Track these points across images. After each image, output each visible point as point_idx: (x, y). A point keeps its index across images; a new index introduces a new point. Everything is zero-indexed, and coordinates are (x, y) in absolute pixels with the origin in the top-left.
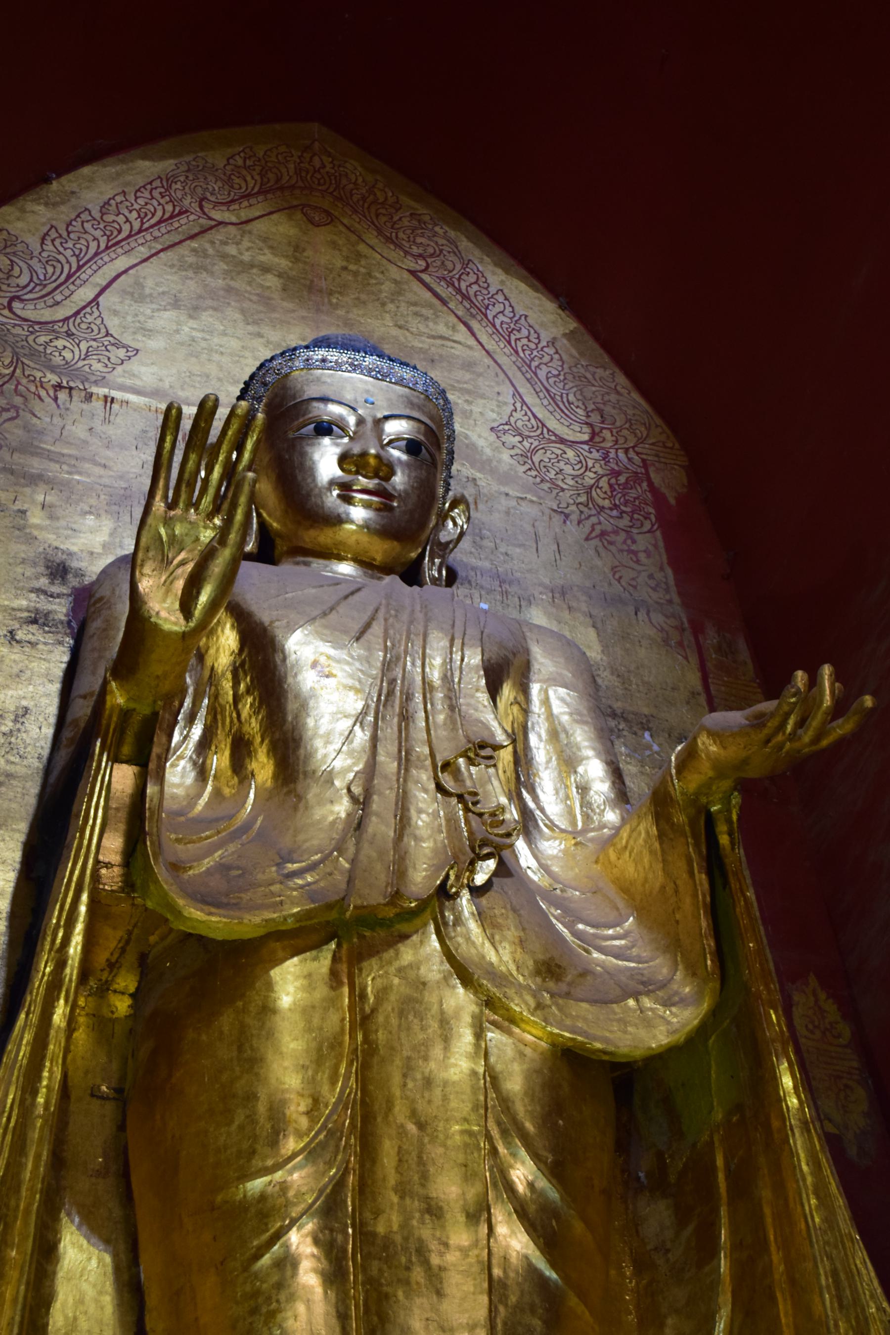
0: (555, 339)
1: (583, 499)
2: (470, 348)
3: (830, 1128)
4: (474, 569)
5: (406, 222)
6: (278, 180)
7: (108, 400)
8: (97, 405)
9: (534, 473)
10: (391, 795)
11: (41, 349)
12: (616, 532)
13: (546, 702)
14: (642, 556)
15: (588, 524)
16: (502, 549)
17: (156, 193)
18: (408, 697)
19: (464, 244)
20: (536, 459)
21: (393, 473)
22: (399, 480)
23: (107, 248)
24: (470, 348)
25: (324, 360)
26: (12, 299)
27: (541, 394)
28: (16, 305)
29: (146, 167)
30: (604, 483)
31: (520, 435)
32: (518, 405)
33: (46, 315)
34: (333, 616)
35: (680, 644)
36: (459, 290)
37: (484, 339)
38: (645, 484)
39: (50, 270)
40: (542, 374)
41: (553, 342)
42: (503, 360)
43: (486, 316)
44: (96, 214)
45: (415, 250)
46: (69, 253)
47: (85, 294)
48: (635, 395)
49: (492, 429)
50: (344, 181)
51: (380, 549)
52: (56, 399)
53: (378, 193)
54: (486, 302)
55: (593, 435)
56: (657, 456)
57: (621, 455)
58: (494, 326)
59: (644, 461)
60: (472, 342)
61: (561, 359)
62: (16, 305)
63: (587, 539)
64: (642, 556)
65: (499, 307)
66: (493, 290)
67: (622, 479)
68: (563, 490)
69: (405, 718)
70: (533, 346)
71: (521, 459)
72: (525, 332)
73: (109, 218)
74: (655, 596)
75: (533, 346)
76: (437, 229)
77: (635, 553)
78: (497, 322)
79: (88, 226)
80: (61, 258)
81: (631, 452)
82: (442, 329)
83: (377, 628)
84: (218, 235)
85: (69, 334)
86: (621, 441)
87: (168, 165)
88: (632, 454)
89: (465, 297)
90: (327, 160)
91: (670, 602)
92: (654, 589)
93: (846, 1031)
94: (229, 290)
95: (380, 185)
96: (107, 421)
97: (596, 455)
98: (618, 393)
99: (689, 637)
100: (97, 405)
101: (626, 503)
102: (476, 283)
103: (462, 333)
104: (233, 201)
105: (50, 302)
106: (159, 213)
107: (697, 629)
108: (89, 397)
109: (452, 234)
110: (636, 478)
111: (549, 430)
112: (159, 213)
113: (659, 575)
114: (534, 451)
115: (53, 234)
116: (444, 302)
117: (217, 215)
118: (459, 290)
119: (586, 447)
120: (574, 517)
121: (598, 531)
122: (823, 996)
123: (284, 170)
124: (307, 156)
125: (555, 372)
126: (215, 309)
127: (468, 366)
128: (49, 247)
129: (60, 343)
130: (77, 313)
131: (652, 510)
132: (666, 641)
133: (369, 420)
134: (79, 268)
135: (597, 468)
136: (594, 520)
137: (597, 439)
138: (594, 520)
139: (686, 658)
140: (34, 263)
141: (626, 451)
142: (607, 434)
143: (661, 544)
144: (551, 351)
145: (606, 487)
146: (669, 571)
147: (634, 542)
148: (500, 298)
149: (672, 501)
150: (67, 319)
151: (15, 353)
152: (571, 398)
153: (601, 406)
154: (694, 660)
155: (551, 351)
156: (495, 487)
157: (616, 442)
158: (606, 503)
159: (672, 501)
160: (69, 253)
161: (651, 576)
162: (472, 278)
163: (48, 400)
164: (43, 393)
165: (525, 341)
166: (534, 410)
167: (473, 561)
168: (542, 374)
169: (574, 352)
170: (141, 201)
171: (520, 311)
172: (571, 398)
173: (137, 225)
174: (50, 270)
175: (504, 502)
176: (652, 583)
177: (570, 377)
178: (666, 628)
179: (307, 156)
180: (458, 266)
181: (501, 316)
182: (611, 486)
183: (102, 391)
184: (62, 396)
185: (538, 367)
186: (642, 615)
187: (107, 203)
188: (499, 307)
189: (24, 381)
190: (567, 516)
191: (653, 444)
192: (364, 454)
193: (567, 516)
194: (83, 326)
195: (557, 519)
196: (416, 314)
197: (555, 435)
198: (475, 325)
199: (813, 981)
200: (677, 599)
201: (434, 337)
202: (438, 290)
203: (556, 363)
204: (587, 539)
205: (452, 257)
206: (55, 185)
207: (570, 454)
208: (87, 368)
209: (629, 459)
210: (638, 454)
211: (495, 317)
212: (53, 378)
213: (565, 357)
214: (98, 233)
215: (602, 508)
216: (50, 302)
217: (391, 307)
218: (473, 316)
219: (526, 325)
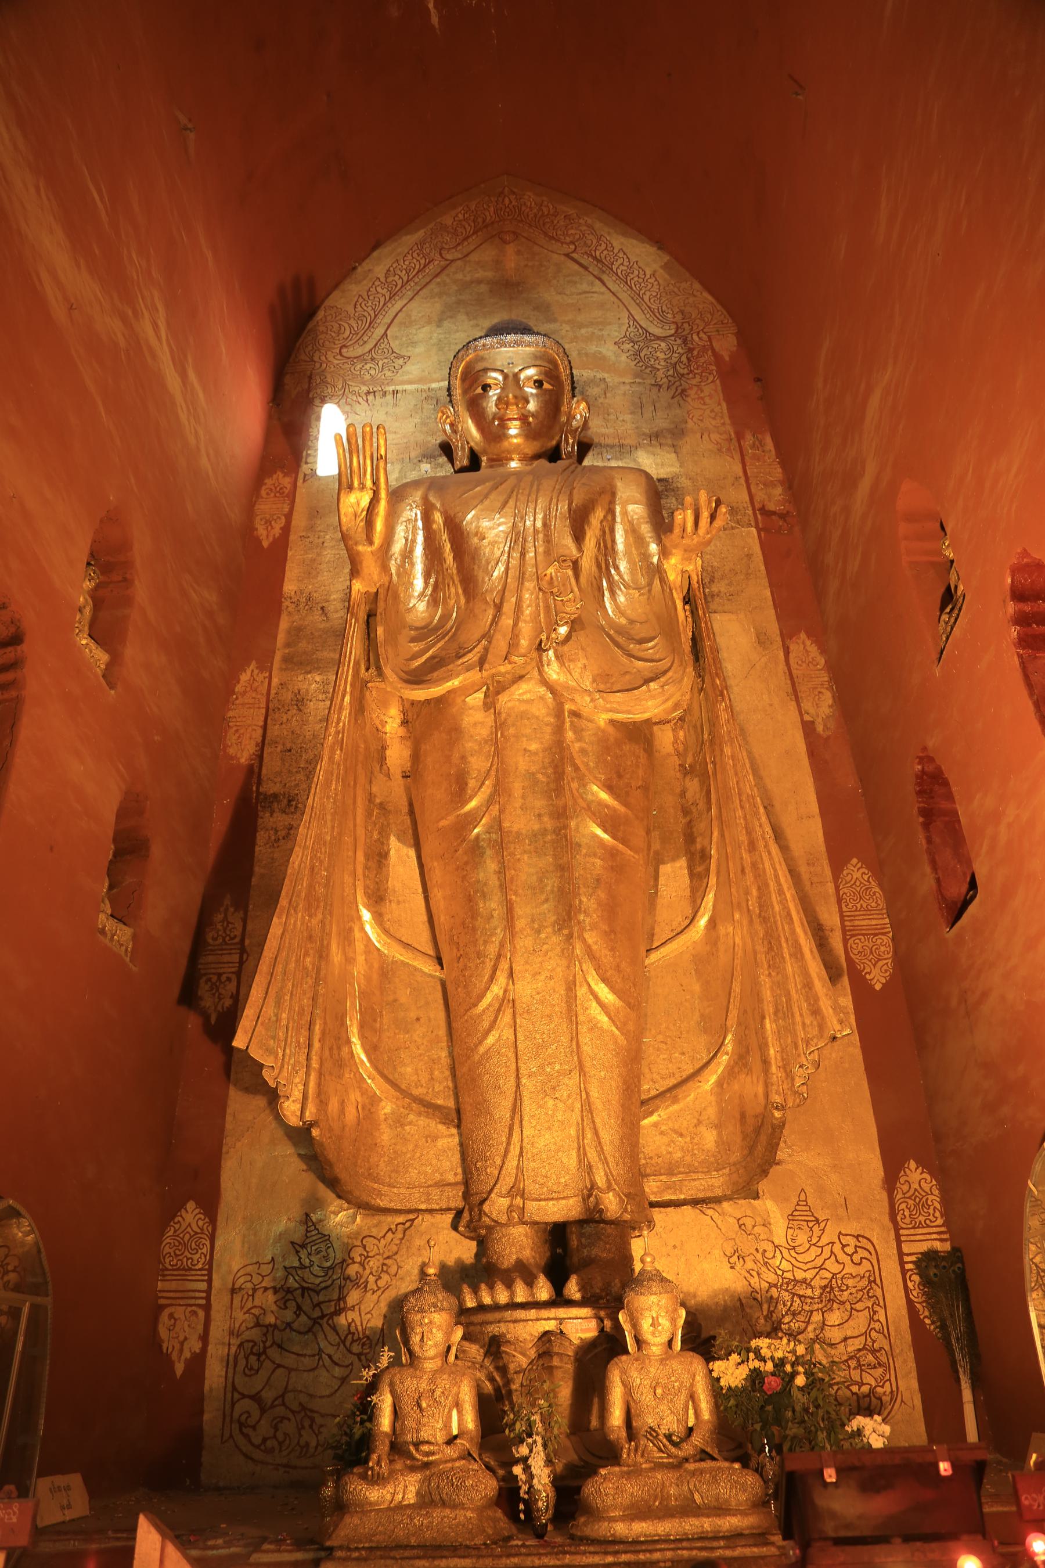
0: (655, 271)
1: (671, 372)
2: (603, 293)
3: (807, 718)
4: (603, 435)
5: (562, 223)
6: (484, 221)
7: (395, 393)
8: (389, 397)
10: (514, 600)
12: (691, 388)
13: (625, 513)
14: (707, 400)
15: (673, 388)
16: (621, 419)
17: (415, 255)
18: (525, 541)
19: (598, 225)
20: (642, 355)
21: (528, 402)
22: (532, 406)
24: (603, 293)
25: (484, 345)
26: (341, 348)
29: (409, 240)
30: (684, 359)
33: (360, 351)
34: (487, 502)
35: (729, 449)
36: (595, 258)
37: (610, 285)
38: (710, 352)
39: (360, 323)
40: (646, 298)
41: (653, 275)
42: (623, 296)
44: (383, 280)
45: (568, 240)
47: (379, 332)
48: (706, 294)
50: (523, 208)
53: (544, 209)
55: (677, 329)
57: (695, 337)
58: (617, 274)
59: (709, 337)
60: (604, 289)
62: (344, 350)
63: (673, 398)
64: (707, 400)
65: (620, 261)
66: (616, 251)
67: (695, 353)
69: (523, 554)
70: (641, 280)
72: (636, 272)
73: (390, 279)
74: (714, 422)
75: (641, 280)
76: (581, 221)
77: (702, 398)
78: (619, 271)
79: (379, 289)
80: (366, 314)
82: (585, 287)
83: (511, 503)
84: (452, 269)
85: (373, 359)
86: (695, 327)
87: (421, 234)
88: (702, 335)
89: (599, 261)
90: (513, 197)
91: (724, 424)
92: (714, 418)
93: (823, 661)
94: (459, 302)
95: (545, 203)
96: (395, 405)
97: (679, 341)
98: (695, 296)
99: (735, 442)
100: (389, 397)
103: (598, 287)
104: (459, 244)
105: (361, 342)
106: (418, 266)
107: (740, 437)
108: (385, 394)
109: (589, 221)
112: (418, 266)
113: (717, 409)
114: (641, 350)
115: (361, 300)
116: (586, 268)
117: (449, 257)
118: (595, 258)
120: (665, 386)
121: (679, 391)
122: (808, 643)
123: (487, 213)
124: (501, 199)
126: (451, 317)
127: (601, 306)
128: (359, 308)
129: (367, 367)
132: (719, 450)
133: (511, 375)
134: (376, 316)
135: (680, 350)
136: (678, 383)
137: (680, 331)
138: (678, 383)
139: (732, 457)
141: (698, 333)
142: (686, 326)
143: (719, 388)
144: (652, 280)
146: (724, 405)
147: (702, 391)
148: (621, 255)
149: (727, 359)
154: (737, 457)
155: (652, 280)
156: (617, 380)
157: (692, 329)
158: (686, 371)
159: (727, 359)
161: (712, 411)
162: (604, 246)
163: (363, 403)
164: (360, 400)
165: (636, 279)
166: (641, 323)
167: (603, 430)
168: (646, 298)
169: (667, 276)
170: (407, 263)
171: (633, 259)
172: (664, 308)
173: (405, 279)
174: (360, 323)
175: (623, 388)
176: (713, 415)
177: (664, 294)
178: (720, 441)
179: (501, 199)
180: (595, 241)
181: (622, 268)
182: (688, 359)
183: (391, 388)
184: (371, 397)
186: (706, 437)
187: (389, 270)
188: (620, 261)
190: (660, 386)
193: (660, 386)
195: (655, 390)
196: (569, 282)
198: (605, 277)
199: (803, 635)
200: (727, 420)
201: (580, 294)
202: (582, 261)
203: (656, 287)
204: (673, 398)
205: (591, 237)
206: (359, 269)
207: (663, 345)
213: (661, 282)
215: (683, 375)
217: (554, 282)
218: (604, 272)
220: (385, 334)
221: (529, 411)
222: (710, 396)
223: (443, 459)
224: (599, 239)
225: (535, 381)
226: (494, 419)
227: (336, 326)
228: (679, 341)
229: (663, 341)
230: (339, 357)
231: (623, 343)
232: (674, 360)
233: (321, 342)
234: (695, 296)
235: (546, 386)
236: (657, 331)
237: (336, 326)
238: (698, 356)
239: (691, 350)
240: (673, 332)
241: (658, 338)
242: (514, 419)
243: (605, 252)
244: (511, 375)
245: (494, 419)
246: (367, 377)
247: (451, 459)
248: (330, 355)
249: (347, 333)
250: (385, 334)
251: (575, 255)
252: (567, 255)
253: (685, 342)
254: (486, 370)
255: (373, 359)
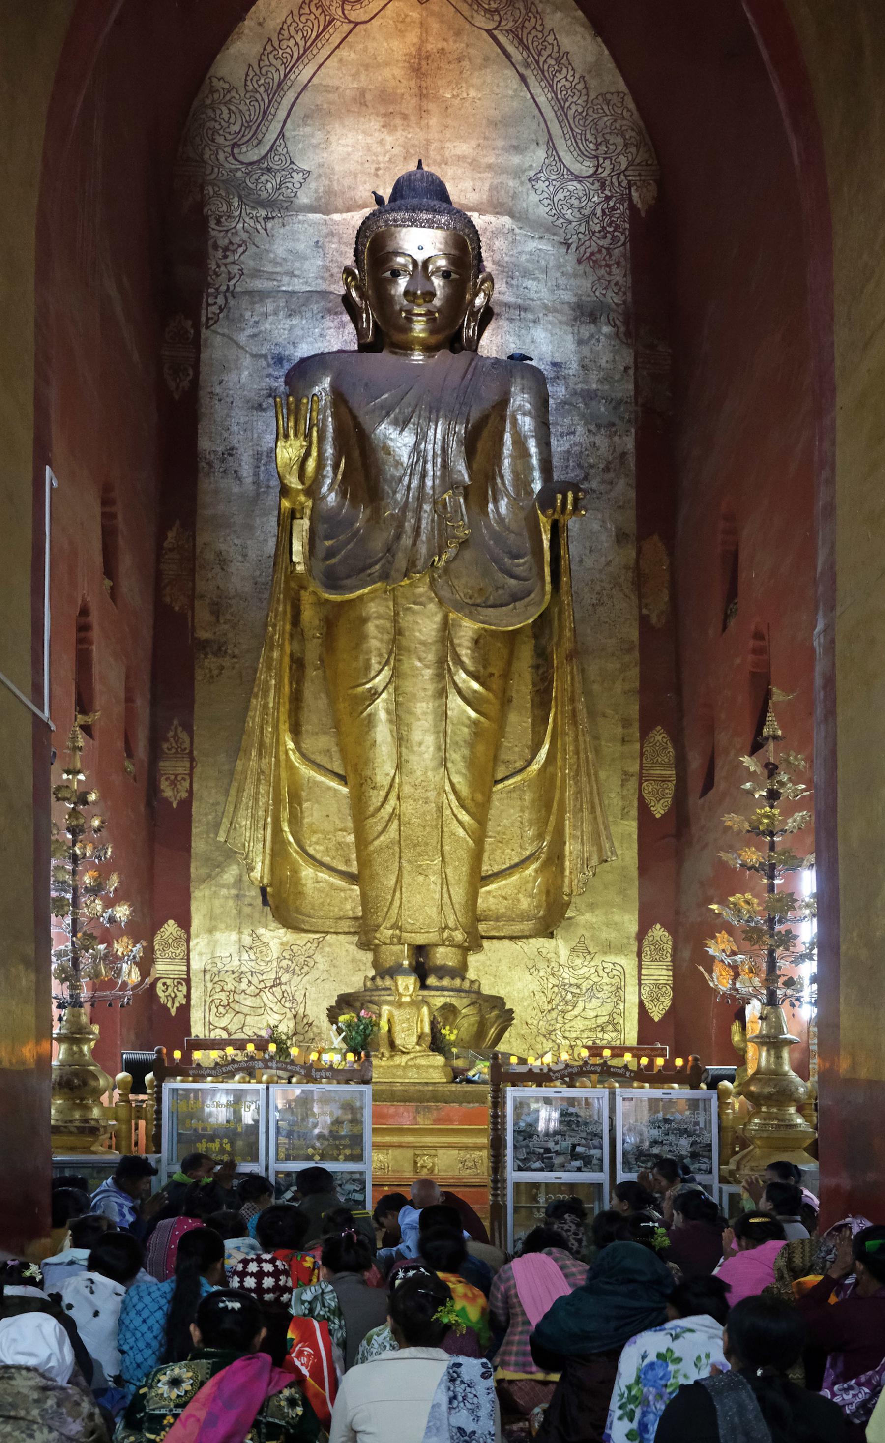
1: (582, 229)
9: (554, 211)
11: (253, 186)
20: (556, 199)
22: (437, 302)
23: (285, 76)
26: (234, 146)
27: (567, 136)
28: (236, 151)
31: (548, 180)
32: (550, 153)
33: (253, 155)
36: (521, 41)
38: (626, 204)
40: (571, 113)
43: (537, 62)
46: (262, 90)
49: (530, 180)
51: (433, 340)
52: (266, 230)
54: (540, 47)
56: (640, 175)
57: (614, 180)
59: (629, 182)
61: (587, 95)
65: (548, 52)
66: (546, 33)
67: (611, 203)
68: (570, 222)
71: (546, 202)
72: (565, 70)
73: (284, 44)
75: (568, 85)
78: (546, 68)
80: (258, 96)
81: (622, 177)
85: (269, 170)
88: (622, 177)
92: (616, 293)
98: (624, 118)
101: (610, 225)
102: (534, 27)
110: (621, 201)
111: (568, 170)
114: (555, 194)
115: (251, 73)
118: (521, 41)
119: (591, 180)
120: (574, 246)
121: (587, 254)
125: (580, 110)
128: (250, 88)
129: (264, 178)
130: (272, 148)
131: (627, 226)
133: (420, 264)
135: (596, 198)
136: (587, 243)
137: (600, 170)
138: (587, 243)
140: (243, 107)
142: (608, 162)
145: (599, 213)
148: (550, 39)
149: (643, 214)
150: (267, 154)
151: (240, 198)
152: (588, 136)
153: (608, 137)
160: (262, 90)
161: (616, 284)
163: (262, 231)
164: (259, 227)
168: (571, 113)
172: (588, 136)
177: (590, 112)
182: (603, 211)
184: (269, 225)
185: (569, 107)
189: (247, 220)
190: (569, 246)
191: (639, 164)
192: (416, 293)
194: (277, 158)
195: (563, 250)
197: (572, 173)
198: (528, 73)
207: (579, 186)
208: (281, 197)
209: (619, 184)
210: (626, 176)
211: (545, 61)
212: (263, 213)
214: (277, 63)
216: (255, 142)
218: (527, 66)
219: (566, 63)
220: (281, 134)
221: (435, 307)
222: (618, 263)
223: (346, 318)
224: (528, 10)
225: (444, 272)
226: (401, 310)
227: (225, 111)
228: (597, 185)
229: (580, 182)
230: (230, 159)
231: (538, 179)
232: (587, 212)
233: (210, 132)
234: (624, 118)
235: (454, 276)
236: (576, 168)
237: (225, 115)
238: (613, 209)
239: (608, 198)
240: (591, 171)
241: (578, 178)
242: (420, 315)
243: (534, 33)
244: (420, 264)
245: (401, 310)
246: (264, 195)
247: (355, 319)
248: (221, 156)
249: (238, 124)
250: (281, 134)
251: (495, 32)
252: (489, 32)
253: (603, 186)
254: (398, 254)
255: (269, 170)
